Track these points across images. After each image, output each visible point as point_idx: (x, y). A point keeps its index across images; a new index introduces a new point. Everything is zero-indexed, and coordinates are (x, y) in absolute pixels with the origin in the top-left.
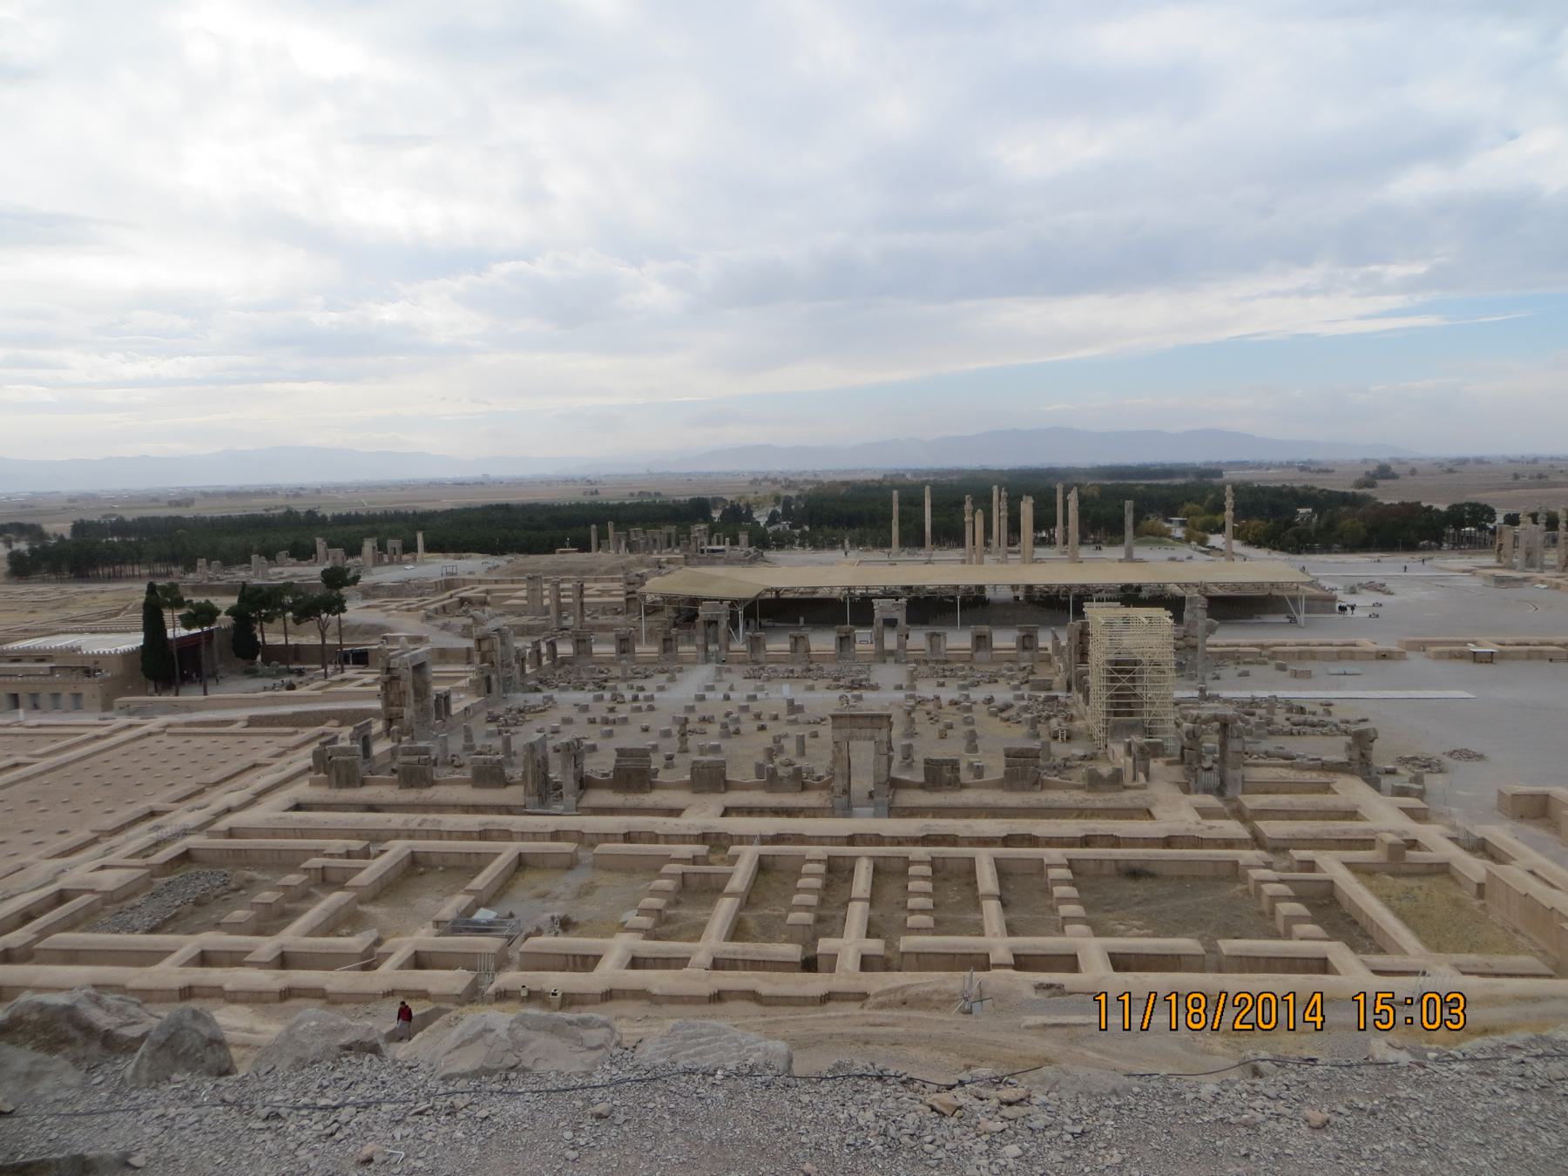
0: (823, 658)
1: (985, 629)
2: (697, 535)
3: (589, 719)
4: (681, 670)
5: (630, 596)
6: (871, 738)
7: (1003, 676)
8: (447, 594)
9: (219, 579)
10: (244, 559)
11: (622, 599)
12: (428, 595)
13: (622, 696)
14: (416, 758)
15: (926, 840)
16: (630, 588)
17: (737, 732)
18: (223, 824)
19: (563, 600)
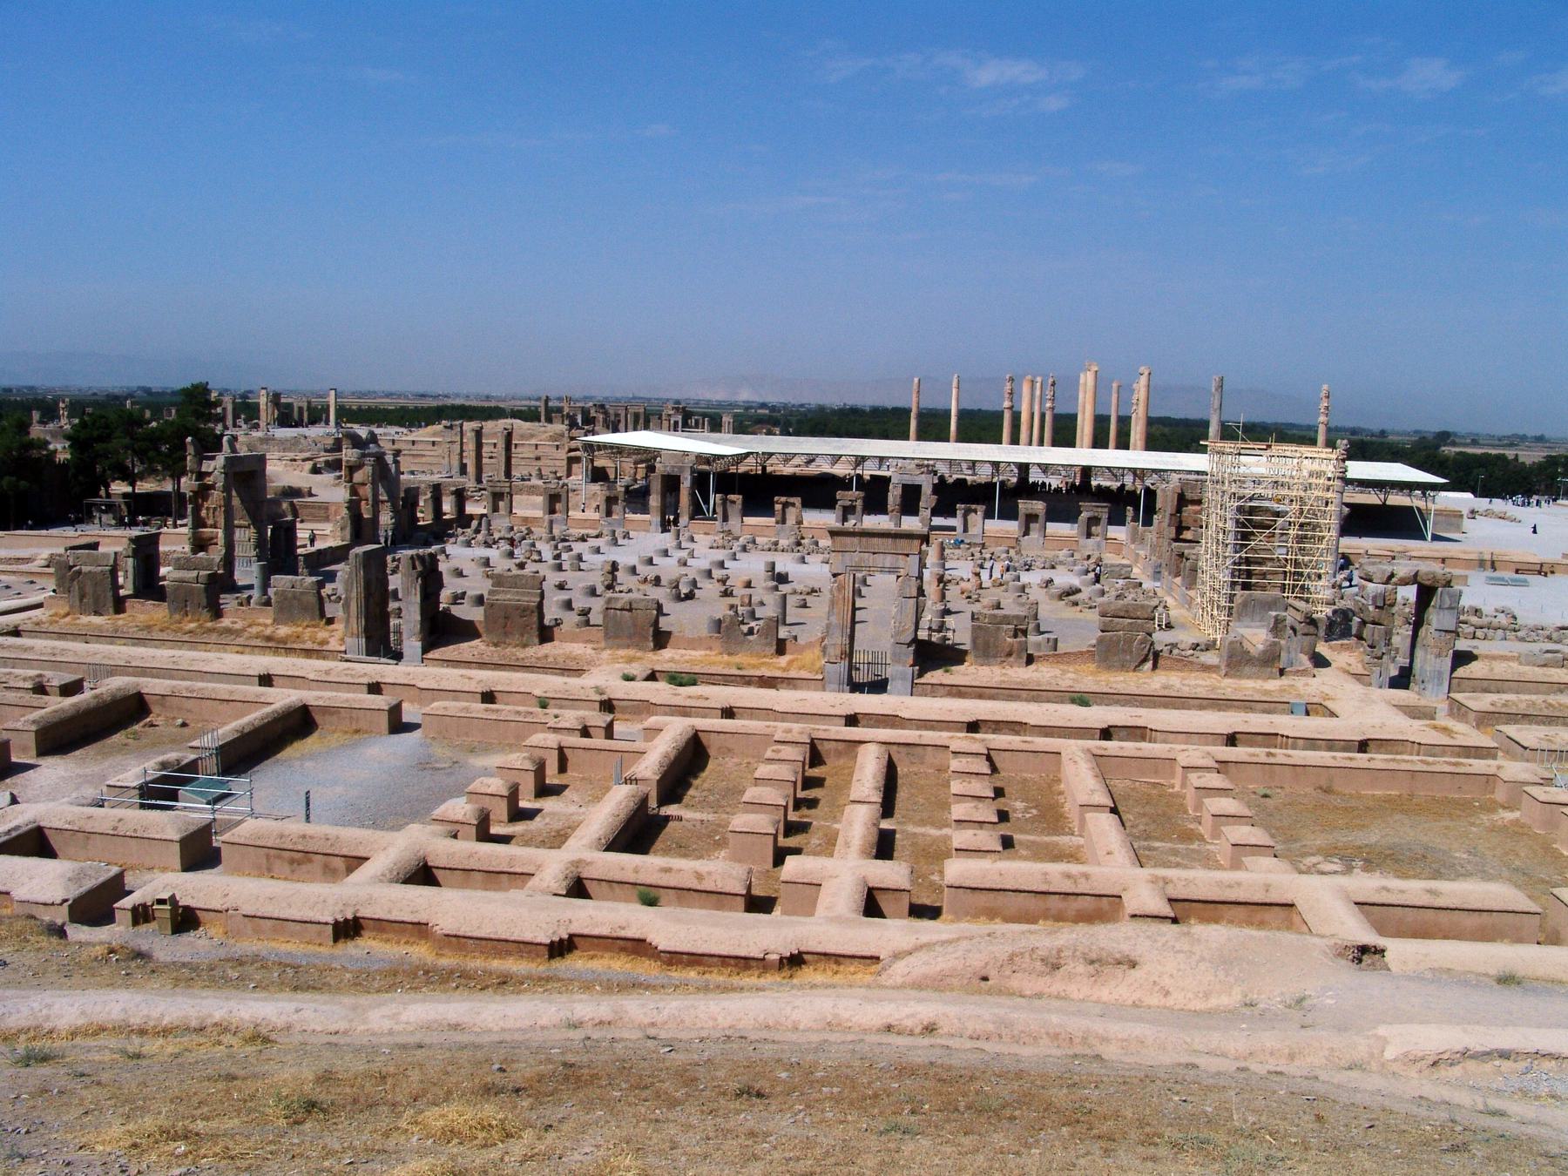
2: (671, 412)
4: (626, 536)
5: (572, 454)
6: (892, 570)
7: (1061, 563)
12: (326, 451)
13: (539, 553)
14: (194, 573)
15: (973, 727)
17: (690, 596)
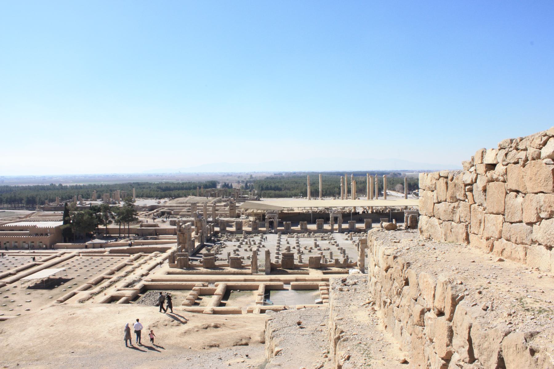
0: (315, 232)
1: (370, 220)
3: (245, 249)
8: (155, 210)
11: (228, 212)
14: (210, 257)
16: (232, 208)
19: (208, 212)
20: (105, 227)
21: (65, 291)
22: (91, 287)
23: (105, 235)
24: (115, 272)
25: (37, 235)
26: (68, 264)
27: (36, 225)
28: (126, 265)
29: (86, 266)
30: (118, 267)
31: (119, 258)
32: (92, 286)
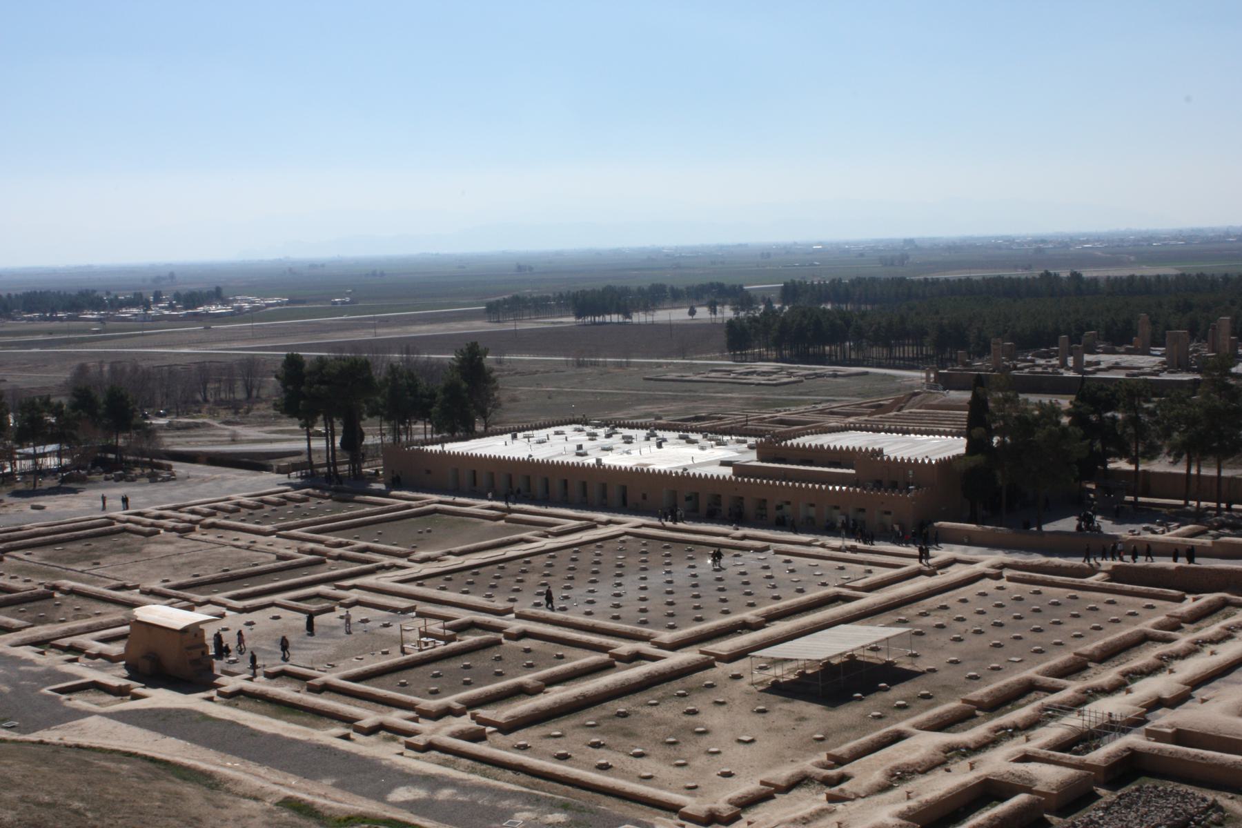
9: (1015, 368)
10: (1039, 341)
18: (1164, 720)
20: (1132, 468)
21: (879, 717)
22: (974, 716)
23: (1129, 498)
24: (1091, 664)
25: (878, 484)
26: (944, 608)
27: (881, 451)
28: (1144, 639)
29: (1001, 625)
30: (1106, 645)
31: (1130, 605)
32: (977, 712)
